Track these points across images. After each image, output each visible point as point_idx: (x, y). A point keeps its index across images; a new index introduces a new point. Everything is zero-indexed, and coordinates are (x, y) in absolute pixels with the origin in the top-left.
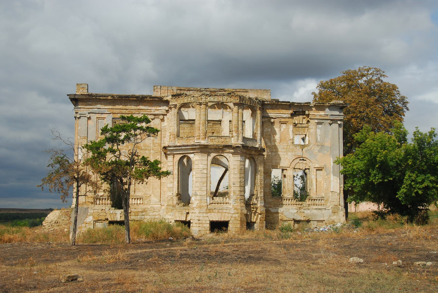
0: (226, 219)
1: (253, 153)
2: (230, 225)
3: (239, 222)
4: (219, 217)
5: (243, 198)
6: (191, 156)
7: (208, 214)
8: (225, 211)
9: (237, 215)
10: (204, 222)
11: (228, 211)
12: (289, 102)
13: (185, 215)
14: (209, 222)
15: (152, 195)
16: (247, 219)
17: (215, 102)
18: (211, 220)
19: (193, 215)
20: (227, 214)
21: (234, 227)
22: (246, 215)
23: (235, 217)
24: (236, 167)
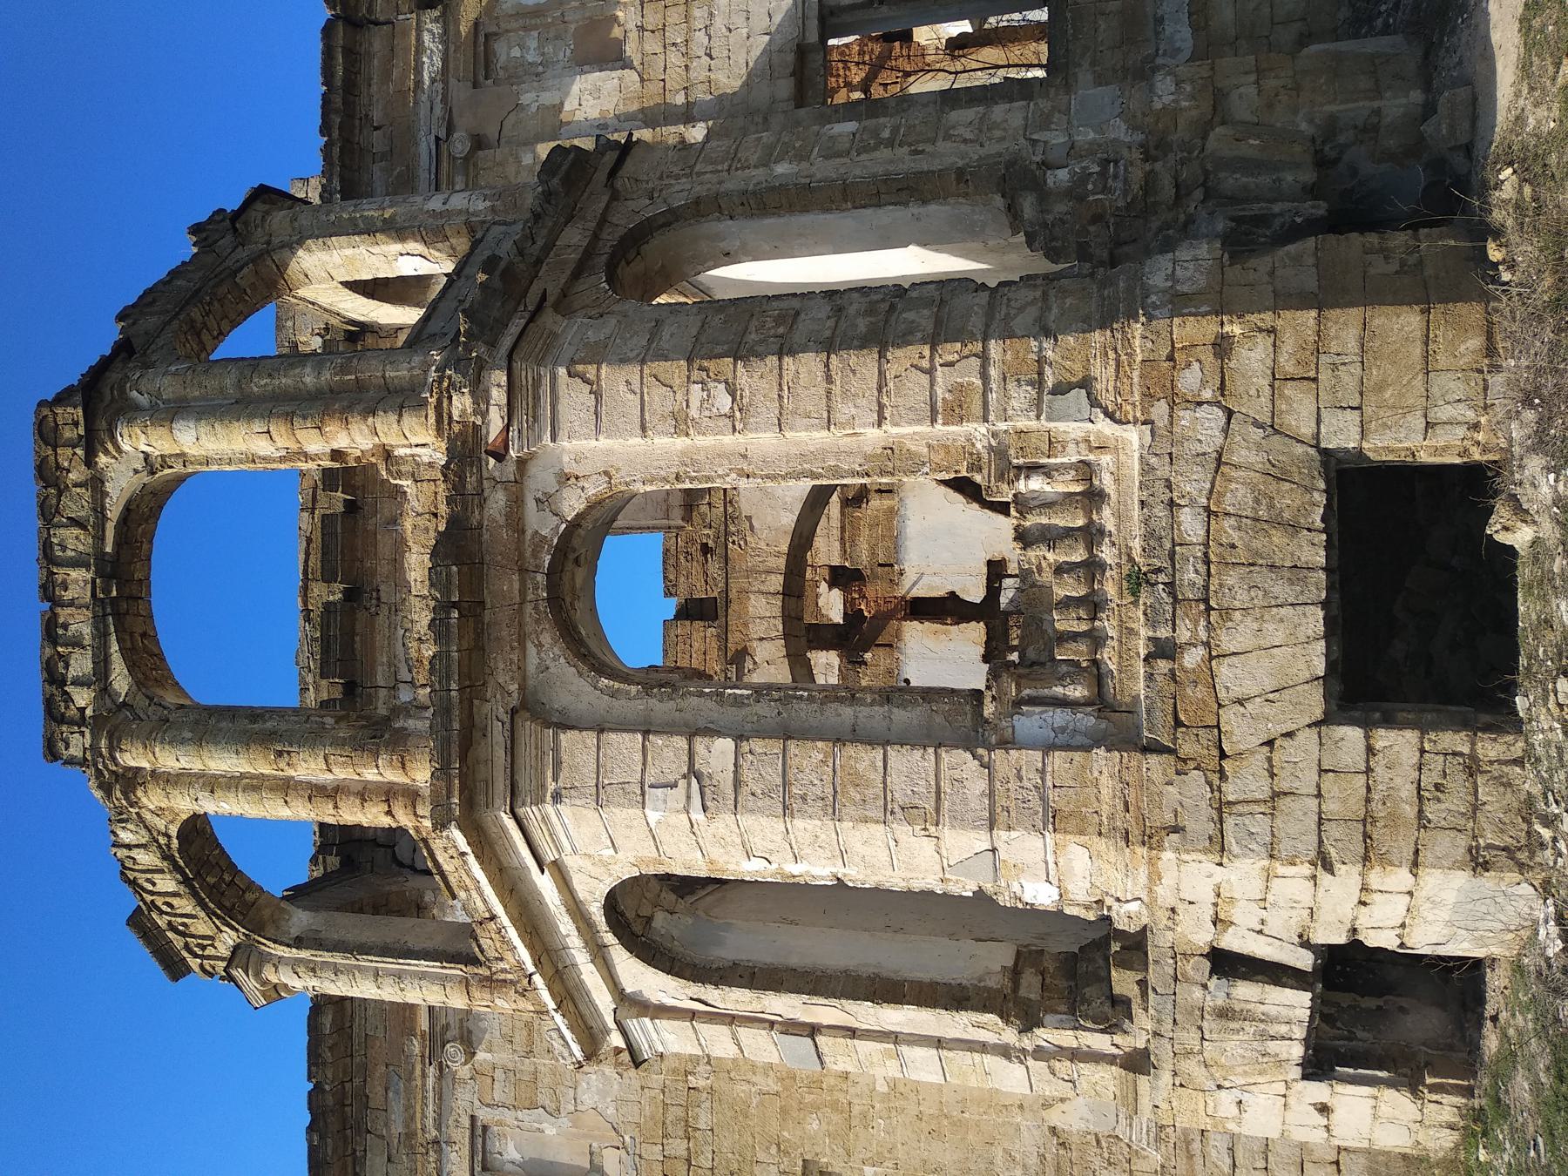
0: (1311, 503)
1: (574, 237)
2: (1399, 439)
3: (1345, 327)
4: (1282, 590)
5: (1026, 295)
6: (593, 892)
7: (1241, 731)
8: (1191, 525)
9: (1252, 358)
10: (1343, 797)
11: (1193, 483)
12: (328, 31)
13: (1246, 991)
14: (1352, 735)
15: (1055, 1117)
16: (1293, 233)
17: (101, 635)
18: (1314, 702)
19: (1244, 915)
20: (1237, 496)
21: (1411, 389)
22: (1242, 242)
23: (1277, 379)
24: (659, 399)
